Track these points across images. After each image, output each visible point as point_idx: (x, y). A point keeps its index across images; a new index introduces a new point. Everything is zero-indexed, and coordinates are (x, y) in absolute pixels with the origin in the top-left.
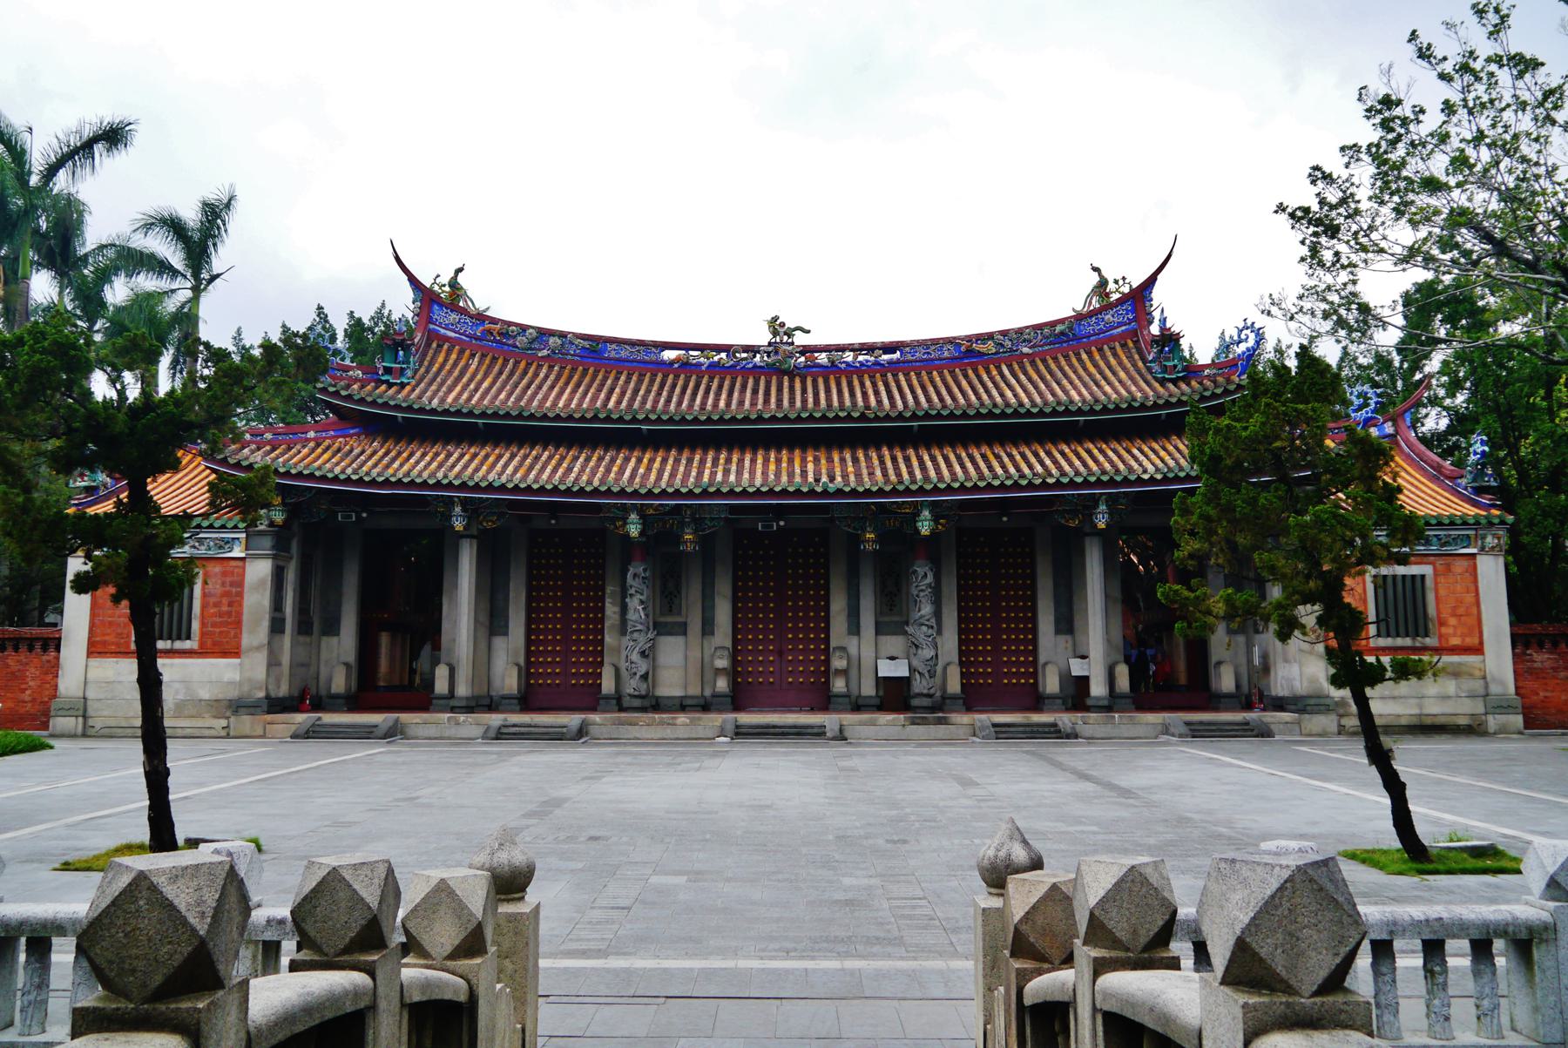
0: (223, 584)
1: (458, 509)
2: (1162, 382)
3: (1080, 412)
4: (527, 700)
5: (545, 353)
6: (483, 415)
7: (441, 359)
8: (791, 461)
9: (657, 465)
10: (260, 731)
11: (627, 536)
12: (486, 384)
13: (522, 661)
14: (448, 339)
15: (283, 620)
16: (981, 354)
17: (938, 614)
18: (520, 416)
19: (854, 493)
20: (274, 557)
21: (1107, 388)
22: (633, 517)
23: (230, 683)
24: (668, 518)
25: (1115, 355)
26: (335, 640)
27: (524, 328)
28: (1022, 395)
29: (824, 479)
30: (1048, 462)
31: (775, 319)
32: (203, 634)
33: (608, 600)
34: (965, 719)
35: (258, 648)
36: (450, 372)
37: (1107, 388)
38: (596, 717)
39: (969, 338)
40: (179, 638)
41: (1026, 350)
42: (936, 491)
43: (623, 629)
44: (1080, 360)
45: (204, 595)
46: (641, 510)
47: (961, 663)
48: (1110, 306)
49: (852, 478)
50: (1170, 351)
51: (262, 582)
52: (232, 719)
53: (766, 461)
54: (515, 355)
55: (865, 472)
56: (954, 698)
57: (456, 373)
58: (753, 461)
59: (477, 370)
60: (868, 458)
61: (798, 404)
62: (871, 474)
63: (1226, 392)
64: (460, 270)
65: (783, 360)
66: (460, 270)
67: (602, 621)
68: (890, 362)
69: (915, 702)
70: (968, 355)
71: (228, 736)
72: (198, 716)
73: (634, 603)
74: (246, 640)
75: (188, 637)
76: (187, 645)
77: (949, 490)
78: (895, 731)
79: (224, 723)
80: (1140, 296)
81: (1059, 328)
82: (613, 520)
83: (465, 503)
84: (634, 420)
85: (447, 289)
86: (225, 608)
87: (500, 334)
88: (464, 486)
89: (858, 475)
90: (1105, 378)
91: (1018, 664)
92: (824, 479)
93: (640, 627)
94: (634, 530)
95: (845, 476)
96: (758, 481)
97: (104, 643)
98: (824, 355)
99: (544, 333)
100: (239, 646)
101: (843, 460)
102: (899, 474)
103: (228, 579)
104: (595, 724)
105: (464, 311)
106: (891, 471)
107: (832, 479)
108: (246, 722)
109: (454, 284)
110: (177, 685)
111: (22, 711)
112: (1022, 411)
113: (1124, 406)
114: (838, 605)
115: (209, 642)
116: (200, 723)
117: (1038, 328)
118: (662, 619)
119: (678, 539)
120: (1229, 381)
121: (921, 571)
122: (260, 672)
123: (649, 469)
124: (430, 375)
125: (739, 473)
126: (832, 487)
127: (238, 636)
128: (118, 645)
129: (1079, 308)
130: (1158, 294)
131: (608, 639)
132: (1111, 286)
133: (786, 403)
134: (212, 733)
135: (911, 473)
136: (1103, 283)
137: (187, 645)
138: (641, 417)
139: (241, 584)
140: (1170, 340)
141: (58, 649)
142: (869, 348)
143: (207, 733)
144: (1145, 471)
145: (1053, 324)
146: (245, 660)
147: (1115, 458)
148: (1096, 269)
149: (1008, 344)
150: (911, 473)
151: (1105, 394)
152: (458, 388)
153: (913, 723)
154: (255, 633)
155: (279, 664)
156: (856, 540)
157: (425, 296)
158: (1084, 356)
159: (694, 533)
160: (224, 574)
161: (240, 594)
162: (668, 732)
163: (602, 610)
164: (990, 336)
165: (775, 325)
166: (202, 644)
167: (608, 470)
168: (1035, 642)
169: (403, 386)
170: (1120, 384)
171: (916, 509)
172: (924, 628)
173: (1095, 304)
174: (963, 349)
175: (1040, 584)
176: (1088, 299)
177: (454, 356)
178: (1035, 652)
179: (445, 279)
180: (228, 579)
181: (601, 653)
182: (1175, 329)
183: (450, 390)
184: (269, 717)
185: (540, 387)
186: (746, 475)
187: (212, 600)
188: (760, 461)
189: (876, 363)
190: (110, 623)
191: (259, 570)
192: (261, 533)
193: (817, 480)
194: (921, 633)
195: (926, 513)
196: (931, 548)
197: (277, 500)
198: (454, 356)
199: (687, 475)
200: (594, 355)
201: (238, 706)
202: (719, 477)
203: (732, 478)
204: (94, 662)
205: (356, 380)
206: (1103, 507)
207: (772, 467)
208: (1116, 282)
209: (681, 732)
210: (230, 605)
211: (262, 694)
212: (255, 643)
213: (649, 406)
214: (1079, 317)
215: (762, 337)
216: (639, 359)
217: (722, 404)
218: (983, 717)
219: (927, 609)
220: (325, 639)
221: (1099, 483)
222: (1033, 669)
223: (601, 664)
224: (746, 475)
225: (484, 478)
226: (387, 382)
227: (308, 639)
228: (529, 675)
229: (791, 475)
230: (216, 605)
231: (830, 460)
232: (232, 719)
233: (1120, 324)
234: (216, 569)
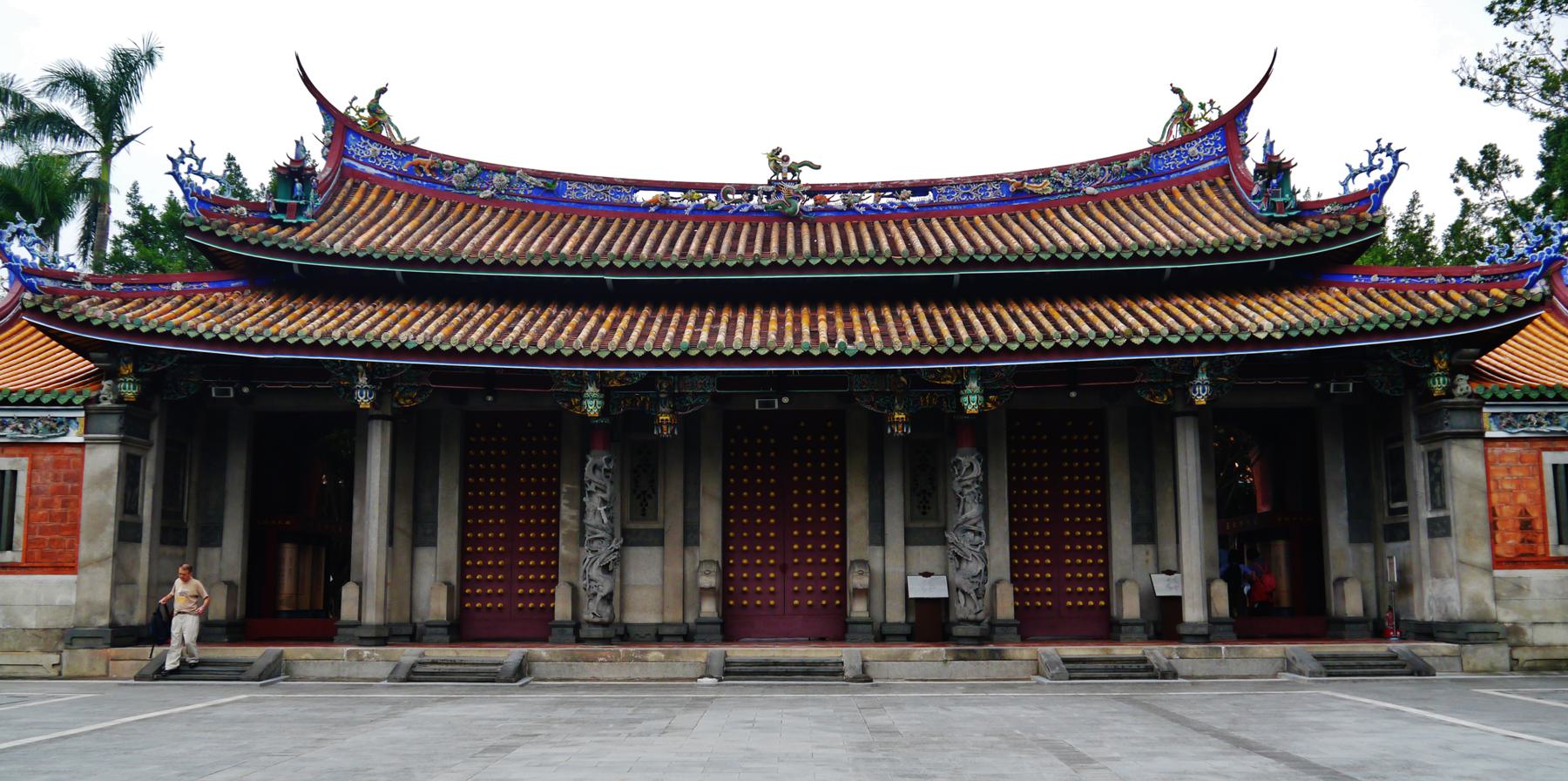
0: (56, 478)
1: (363, 380)
2: (1270, 222)
3: (1168, 258)
4: (459, 630)
5: (488, 193)
6: (401, 262)
7: (355, 199)
8: (797, 321)
9: (624, 324)
10: (101, 670)
11: (585, 417)
12: (408, 227)
13: (454, 579)
14: (366, 176)
15: (139, 526)
16: (1034, 195)
17: (985, 516)
18: (447, 264)
19: (880, 357)
20: (123, 443)
21: (1200, 230)
22: (592, 390)
23: (63, 607)
24: (637, 391)
25: (1203, 195)
26: (215, 552)
27: (461, 163)
28: (1093, 238)
29: (841, 339)
30: (1131, 319)
31: (777, 151)
32: (28, 543)
33: (563, 502)
34: (1026, 652)
35: (100, 562)
36: (365, 214)
37: (1200, 230)
38: (541, 651)
39: (1020, 176)
41: (1090, 190)
42: (987, 354)
43: (581, 536)
44: (1158, 201)
46: (602, 381)
47: (1013, 580)
48: (1196, 136)
49: (877, 338)
50: (1279, 185)
51: (106, 475)
52: (66, 654)
53: (765, 321)
54: (448, 195)
55: (893, 332)
56: (1006, 624)
57: (372, 215)
58: (749, 321)
59: (400, 213)
60: (897, 318)
61: (806, 247)
62: (902, 334)
63: (1356, 233)
64: (382, 91)
65: (786, 201)
66: (382, 91)
67: (556, 528)
68: (921, 205)
69: (959, 631)
70: (1018, 195)
71: (60, 677)
72: (21, 650)
73: (594, 503)
74: (85, 551)
75: (10, 547)
77: (1005, 353)
78: (934, 668)
79: (54, 658)
80: (1232, 123)
81: (1131, 163)
82: (567, 396)
83: (372, 371)
84: (595, 268)
85: (366, 114)
86: (58, 509)
87: (431, 170)
88: (367, 349)
89: (885, 336)
90: (1195, 220)
91: (1084, 581)
92: (841, 339)
93: (601, 534)
94: (593, 407)
95: (868, 336)
96: (755, 342)
98: (837, 196)
99: (486, 169)
100: (75, 559)
101: (864, 320)
102: (938, 334)
103: (63, 471)
104: (539, 659)
105: (387, 142)
106: (927, 330)
107: (851, 338)
108: (83, 658)
109: (374, 108)
112: (1095, 256)
113: (1225, 250)
114: (857, 508)
115: (37, 553)
116: (23, 659)
117: (1106, 162)
118: (632, 526)
119: (650, 421)
120: (1359, 220)
121: (965, 461)
122: (103, 593)
123: (613, 329)
124: (339, 217)
125: (730, 333)
126: (851, 350)
127: (74, 546)
129: (1156, 139)
130: (1255, 123)
131: (563, 551)
132: (1196, 112)
133: (790, 247)
135: (954, 332)
136: (1186, 108)
138: (603, 264)
139: (78, 478)
140: (1276, 169)
142: (894, 188)
143: (32, 672)
144: (1260, 329)
145: (1124, 158)
146: (85, 576)
147: (1217, 314)
148: (1176, 91)
149: (1068, 182)
150: (954, 332)
151: (1199, 236)
152: (372, 230)
153: (958, 659)
154: (96, 543)
155: (133, 582)
156: (879, 422)
157: (339, 124)
158: (1164, 197)
159: (673, 412)
160: (57, 464)
161: (78, 491)
162: (636, 670)
163: (557, 514)
164: (1046, 173)
165: (777, 159)
167: (559, 331)
168: (1106, 553)
169: (300, 226)
170: (1213, 225)
171: (961, 377)
172: (970, 535)
173: (1176, 134)
174: (1012, 188)
175: (1113, 480)
176: (1167, 129)
177: (373, 197)
178: (1106, 567)
179: (363, 103)
180: (63, 471)
181: (555, 569)
182: (1286, 156)
183: (361, 233)
184: (114, 651)
185: (476, 232)
186: (739, 335)
187: (41, 499)
188: (757, 319)
189: (904, 207)
191: (103, 460)
192: (105, 412)
193: (832, 341)
194: (965, 542)
195: (973, 385)
196: (976, 430)
197: (127, 369)
198: (373, 197)
199: (661, 335)
200: (550, 194)
201: (72, 637)
202: (704, 337)
203: (721, 338)
205: (239, 219)
206: (1203, 377)
207: (773, 326)
208: (1202, 106)
209: (654, 671)
210: (64, 505)
211: (104, 621)
212: (97, 555)
213: (615, 250)
214: (1156, 150)
215: (760, 174)
216: (608, 200)
217: (709, 249)
218: (1049, 649)
219: (973, 511)
220: (202, 551)
221: (1201, 344)
222: (1105, 586)
223: (556, 581)
224: (739, 335)
225: (395, 338)
226: (279, 222)
227: (179, 551)
228: (463, 597)
229: (798, 336)
230: (46, 505)
231: (848, 320)
232: (66, 654)
233: (1207, 159)
234: (47, 458)
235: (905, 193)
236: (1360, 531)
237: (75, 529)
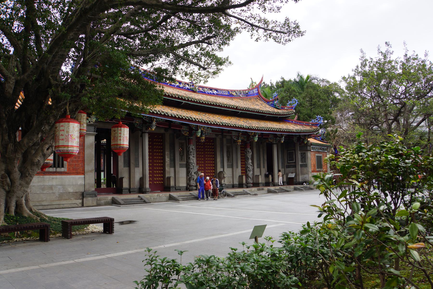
23: (81, 185)
33: (166, 156)
34: (266, 188)
35: (91, 171)
39: (232, 91)
40: (59, 167)
72: (69, 199)
74: (86, 168)
100: (84, 170)
110: (59, 187)
114: (219, 160)
115: (71, 168)
132: (254, 84)
134: (77, 206)
136: (253, 83)
137: (62, 170)
154: (90, 166)
164: (235, 91)
166: (69, 169)
171: (255, 135)
212: (90, 169)
235: (213, 90)
237: (83, 161)
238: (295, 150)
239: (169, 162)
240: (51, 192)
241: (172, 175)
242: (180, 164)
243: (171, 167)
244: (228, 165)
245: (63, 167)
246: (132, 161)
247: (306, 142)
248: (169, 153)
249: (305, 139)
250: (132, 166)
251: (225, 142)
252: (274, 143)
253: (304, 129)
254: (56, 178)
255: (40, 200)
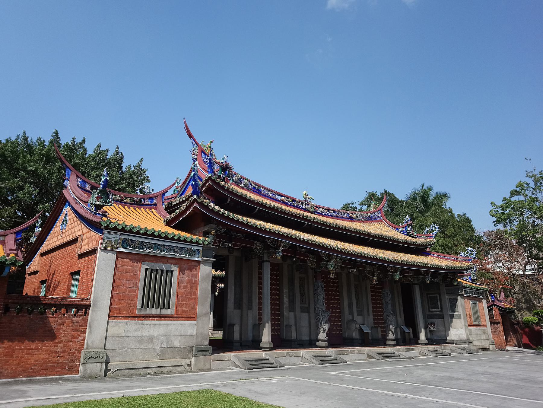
23: (192, 336)
45: (179, 281)
64: (212, 142)
66: (212, 142)
69: (388, 342)
76: (169, 312)
86: (189, 290)
97: (119, 309)
100: (195, 313)
110: (162, 338)
111: (55, 360)
115: (180, 310)
128: (128, 311)
141: (86, 313)
154: (204, 306)
161: (196, 282)
190: (124, 296)
204: (112, 322)
212: (204, 312)
236: (428, 317)
237: (195, 299)
238: (439, 294)
239: (287, 303)
240: (150, 346)
241: (292, 322)
242: (301, 308)
243: (290, 311)
244: (357, 311)
245: (169, 308)
246: (245, 301)
247: (455, 284)
248: (287, 291)
249: (455, 279)
250: (245, 307)
251: (352, 279)
252: (416, 282)
253: (453, 265)
254: (160, 325)
255: (134, 359)
